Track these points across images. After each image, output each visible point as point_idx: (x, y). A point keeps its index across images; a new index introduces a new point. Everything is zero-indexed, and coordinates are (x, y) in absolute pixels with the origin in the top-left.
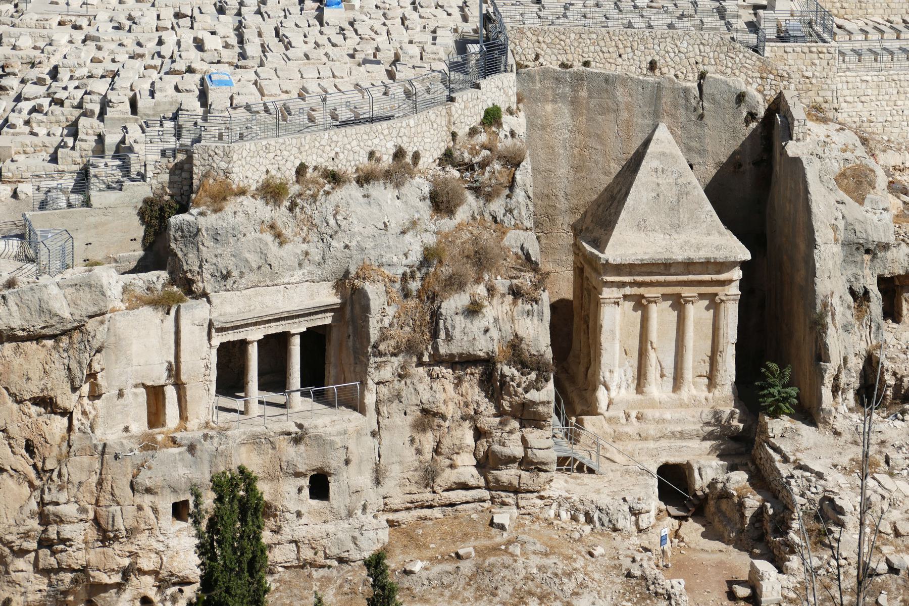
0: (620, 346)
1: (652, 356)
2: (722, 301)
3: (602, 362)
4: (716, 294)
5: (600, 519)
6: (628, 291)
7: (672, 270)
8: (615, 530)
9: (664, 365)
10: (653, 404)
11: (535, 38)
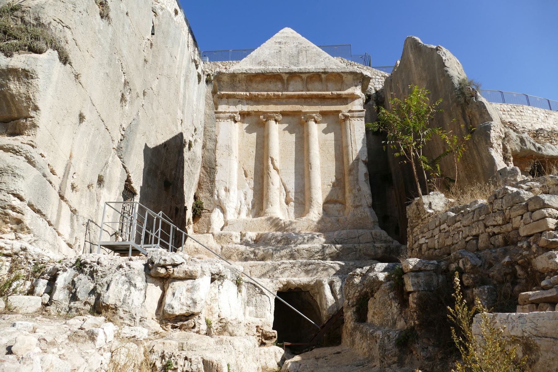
0: (239, 168)
1: (275, 179)
2: (346, 117)
3: (217, 179)
4: (339, 112)
7: (290, 88)
8: (98, 308)
11: (224, 67)
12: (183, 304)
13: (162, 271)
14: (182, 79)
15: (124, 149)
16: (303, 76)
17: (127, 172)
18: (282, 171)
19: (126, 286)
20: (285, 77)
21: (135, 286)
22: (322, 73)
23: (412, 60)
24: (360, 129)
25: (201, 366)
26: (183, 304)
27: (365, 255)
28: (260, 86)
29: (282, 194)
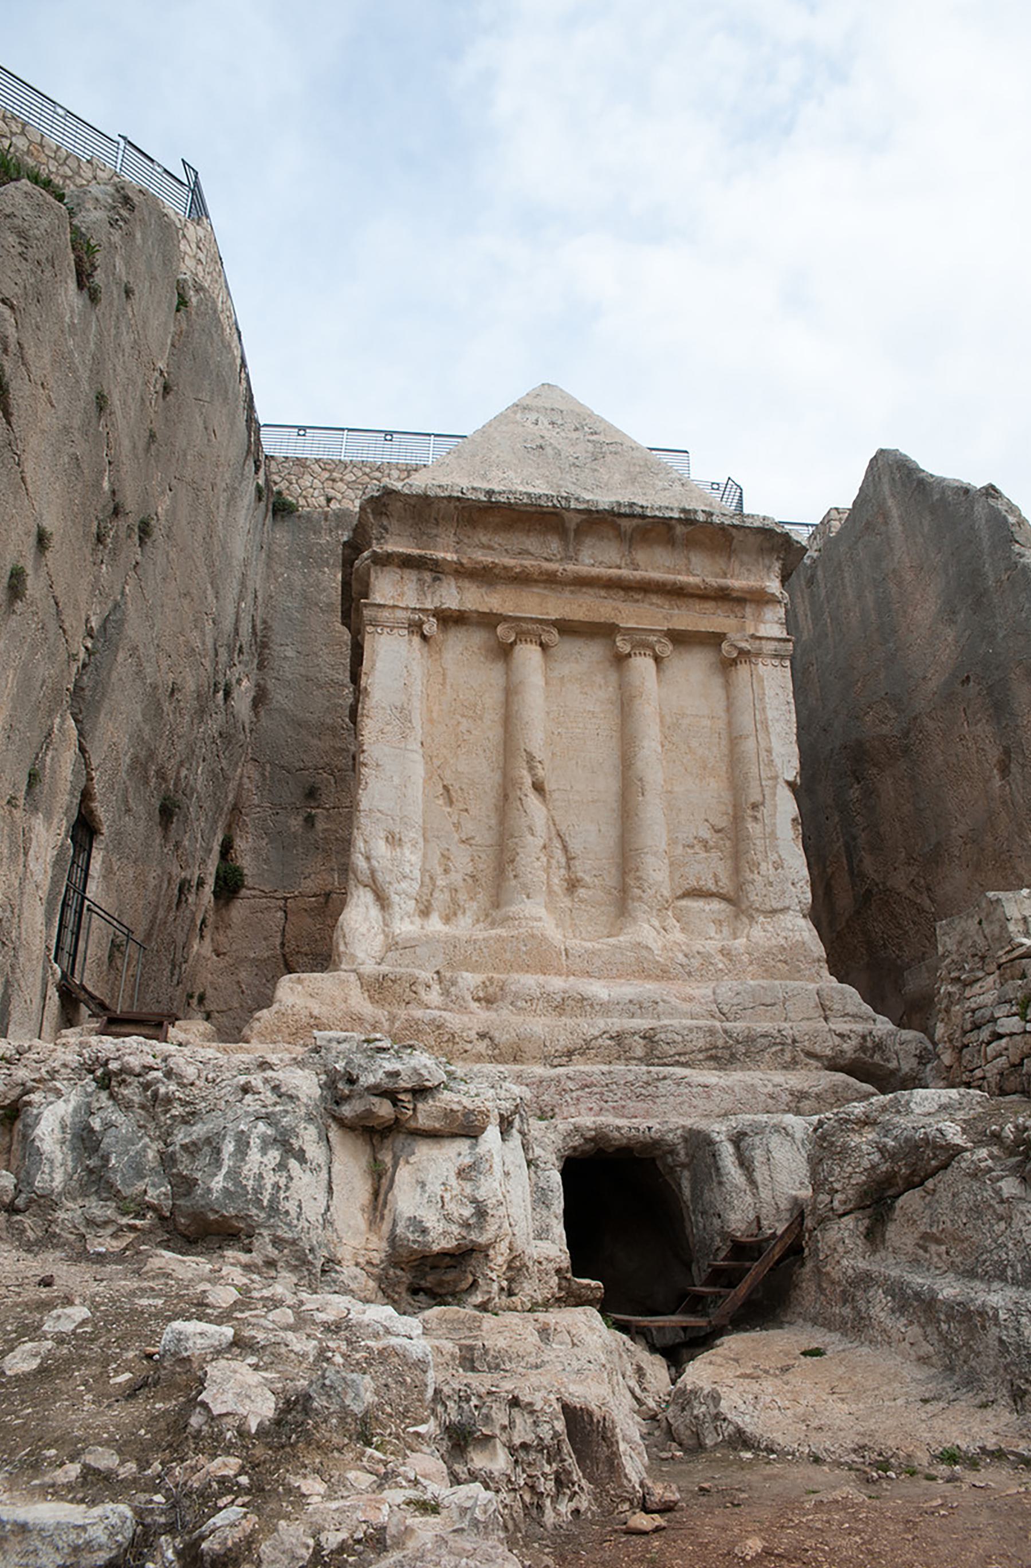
3: (364, 805)
5: (85, 1140)
6: (452, 596)
9: (575, 846)
10: (540, 957)
11: (327, 475)
12: (448, 1218)
13: (384, 1109)
14: (223, 497)
15: (87, 692)
16: (625, 523)
17: (86, 764)
18: (555, 795)
19: (274, 1155)
20: (573, 521)
21: (301, 1156)
22: (679, 520)
23: (895, 513)
24: (779, 691)
25: (560, 1426)
26: (448, 1218)
27: (809, 1054)
28: (497, 540)
29: (553, 862)
